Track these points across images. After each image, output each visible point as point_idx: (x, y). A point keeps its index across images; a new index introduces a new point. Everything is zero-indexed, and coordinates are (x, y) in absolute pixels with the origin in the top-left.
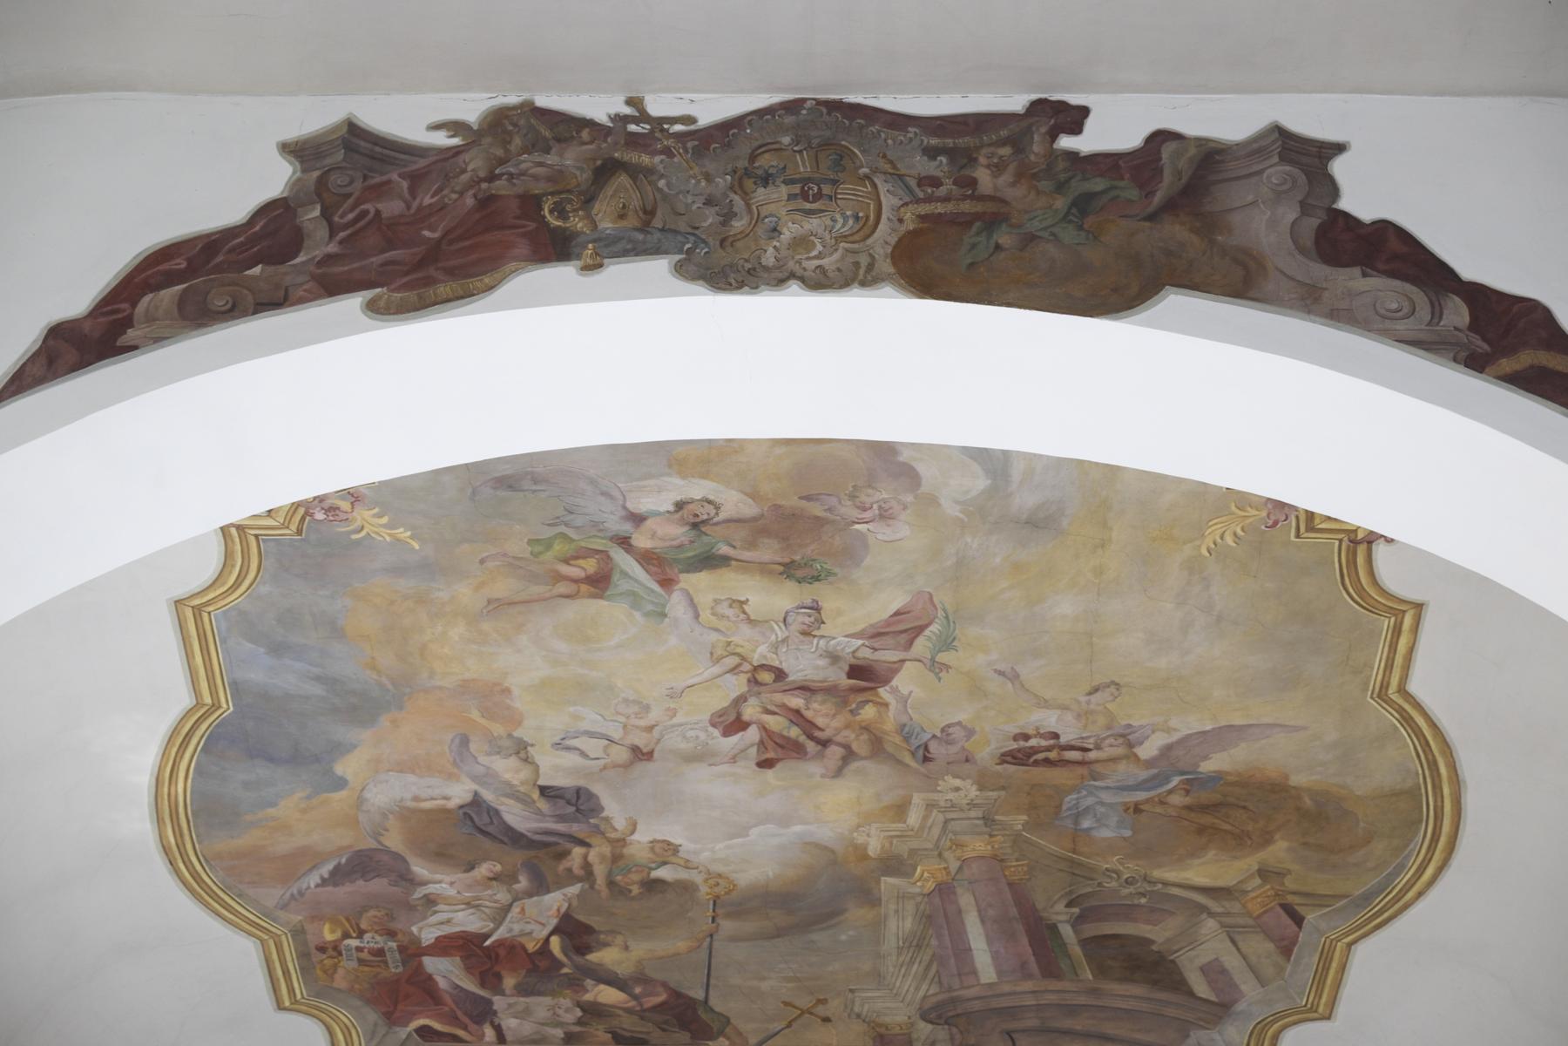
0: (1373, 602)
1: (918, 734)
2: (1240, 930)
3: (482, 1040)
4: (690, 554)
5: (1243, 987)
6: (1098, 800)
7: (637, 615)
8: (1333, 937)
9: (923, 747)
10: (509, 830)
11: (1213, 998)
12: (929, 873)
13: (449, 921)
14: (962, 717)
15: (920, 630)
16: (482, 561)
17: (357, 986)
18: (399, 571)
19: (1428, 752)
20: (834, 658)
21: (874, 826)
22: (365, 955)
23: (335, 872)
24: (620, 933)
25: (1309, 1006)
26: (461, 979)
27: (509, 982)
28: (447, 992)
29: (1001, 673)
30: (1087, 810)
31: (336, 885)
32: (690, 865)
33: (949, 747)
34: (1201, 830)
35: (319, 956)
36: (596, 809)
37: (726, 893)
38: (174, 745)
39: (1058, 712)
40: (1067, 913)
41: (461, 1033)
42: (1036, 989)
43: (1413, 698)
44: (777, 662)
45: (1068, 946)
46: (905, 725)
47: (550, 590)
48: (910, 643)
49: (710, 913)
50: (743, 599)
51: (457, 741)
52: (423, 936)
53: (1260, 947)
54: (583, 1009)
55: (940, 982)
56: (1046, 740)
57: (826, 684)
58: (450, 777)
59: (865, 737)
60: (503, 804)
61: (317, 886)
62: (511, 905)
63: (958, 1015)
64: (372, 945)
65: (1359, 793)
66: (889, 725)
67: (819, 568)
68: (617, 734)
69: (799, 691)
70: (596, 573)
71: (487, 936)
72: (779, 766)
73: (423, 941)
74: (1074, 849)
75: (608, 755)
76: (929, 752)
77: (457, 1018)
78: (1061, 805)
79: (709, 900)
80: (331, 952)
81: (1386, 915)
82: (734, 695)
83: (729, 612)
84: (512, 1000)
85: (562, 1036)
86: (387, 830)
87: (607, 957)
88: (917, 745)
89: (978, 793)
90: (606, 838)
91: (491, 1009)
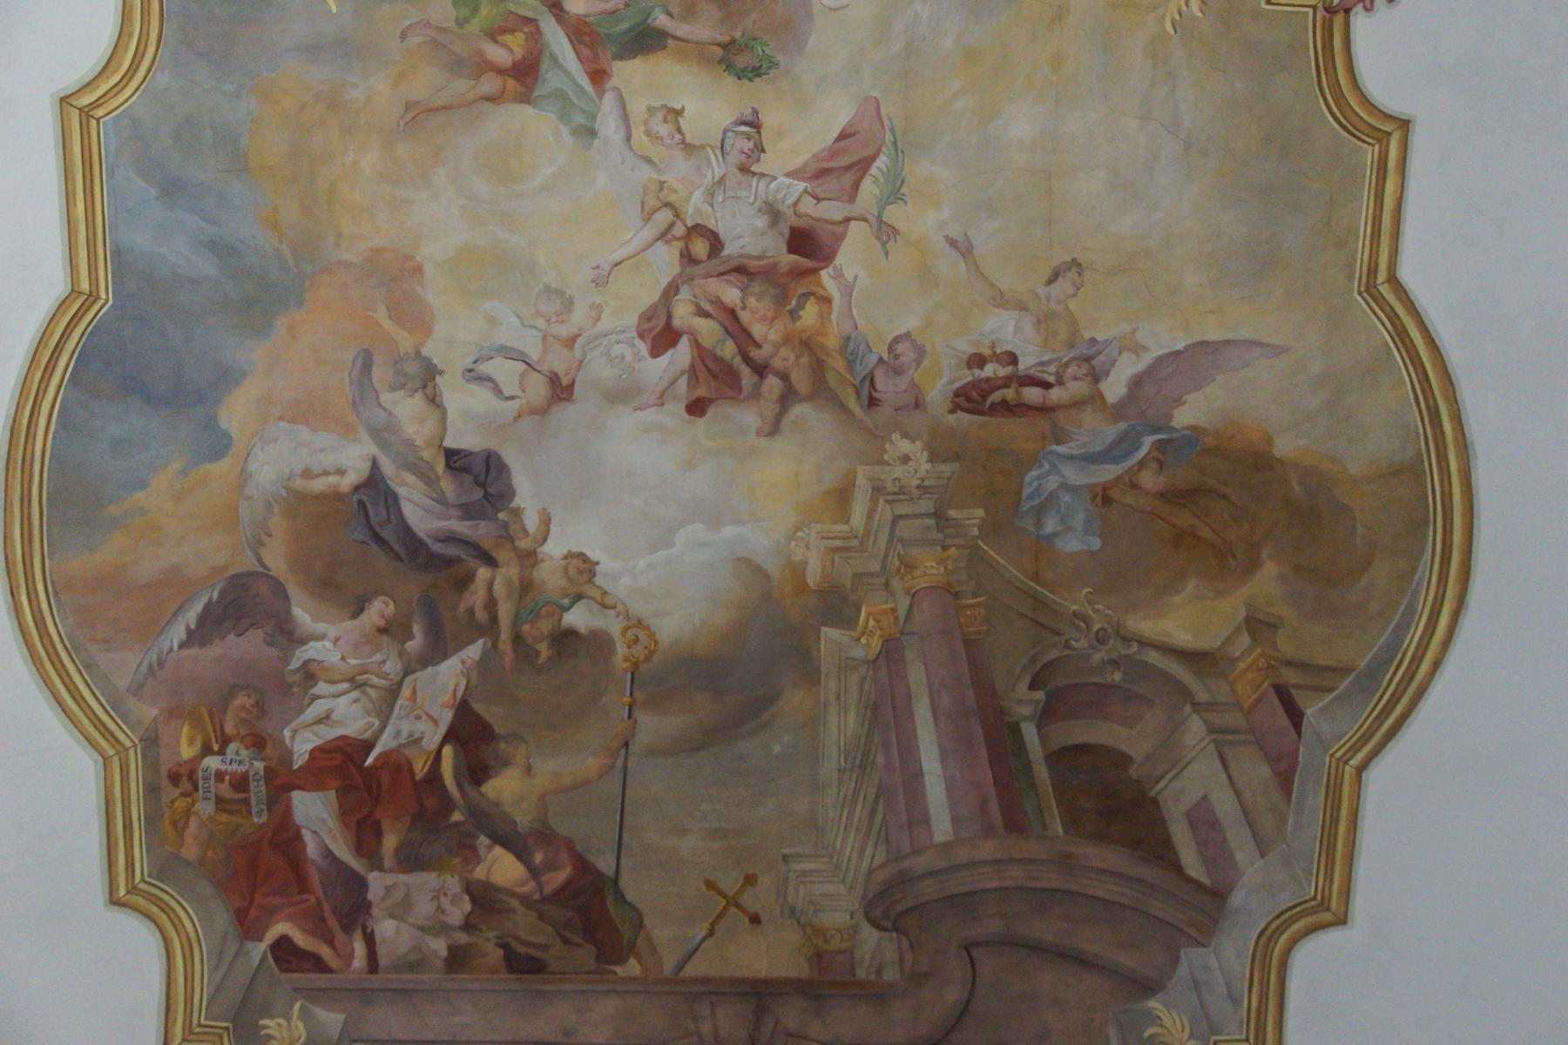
0: (1354, 118)
1: (863, 357)
2: (1230, 737)
3: (349, 965)
4: (625, 26)
5: (1240, 857)
6: (1061, 480)
7: (564, 130)
8: (1338, 755)
9: (868, 380)
10: (407, 531)
11: (1205, 880)
12: (874, 619)
13: (325, 719)
14: (910, 324)
15: (865, 164)
16: (403, 36)
17: (210, 853)
18: (313, 50)
19: (1429, 395)
20: (773, 213)
21: (818, 527)
22: (225, 789)
23: (203, 618)
24: (522, 739)
25: (1319, 897)
26: (334, 836)
27: (390, 842)
28: (314, 863)
29: (953, 243)
30: (1052, 496)
31: (202, 645)
32: (607, 601)
33: (898, 378)
34: (1180, 538)
35: (170, 793)
36: (508, 494)
37: (648, 659)
38: (38, 367)
39: (1015, 314)
40: (1031, 701)
41: (325, 952)
42: (999, 855)
43: (1406, 292)
44: (713, 222)
45: (1034, 766)
46: (848, 339)
47: (474, 87)
48: (856, 186)
49: (626, 699)
50: (678, 107)
51: (359, 363)
52: (295, 749)
53: (1256, 772)
54: (474, 901)
55: (887, 842)
56: (1004, 366)
57: (765, 262)
58: (348, 432)
59: (805, 360)
60: (404, 484)
61: (181, 646)
62: (401, 683)
63: (908, 911)
64: (235, 766)
65: (1352, 471)
66: (832, 342)
67: (761, 53)
68: (534, 354)
69: (736, 274)
70: (524, 58)
71: (369, 746)
72: (711, 412)
73: (296, 756)
74: (1037, 573)
75: (524, 391)
76: (875, 390)
77: (323, 920)
78: (1019, 492)
79: (625, 670)
80: (185, 784)
81: (1399, 709)
82: (664, 282)
83: (664, 130)
84: (390, 879)
85: (444, 953)
86: (269, 535)
87: (504, 787)
88: (862, 375)
89: (928, 466)
90: (515, 548)
91: (365, 899)
